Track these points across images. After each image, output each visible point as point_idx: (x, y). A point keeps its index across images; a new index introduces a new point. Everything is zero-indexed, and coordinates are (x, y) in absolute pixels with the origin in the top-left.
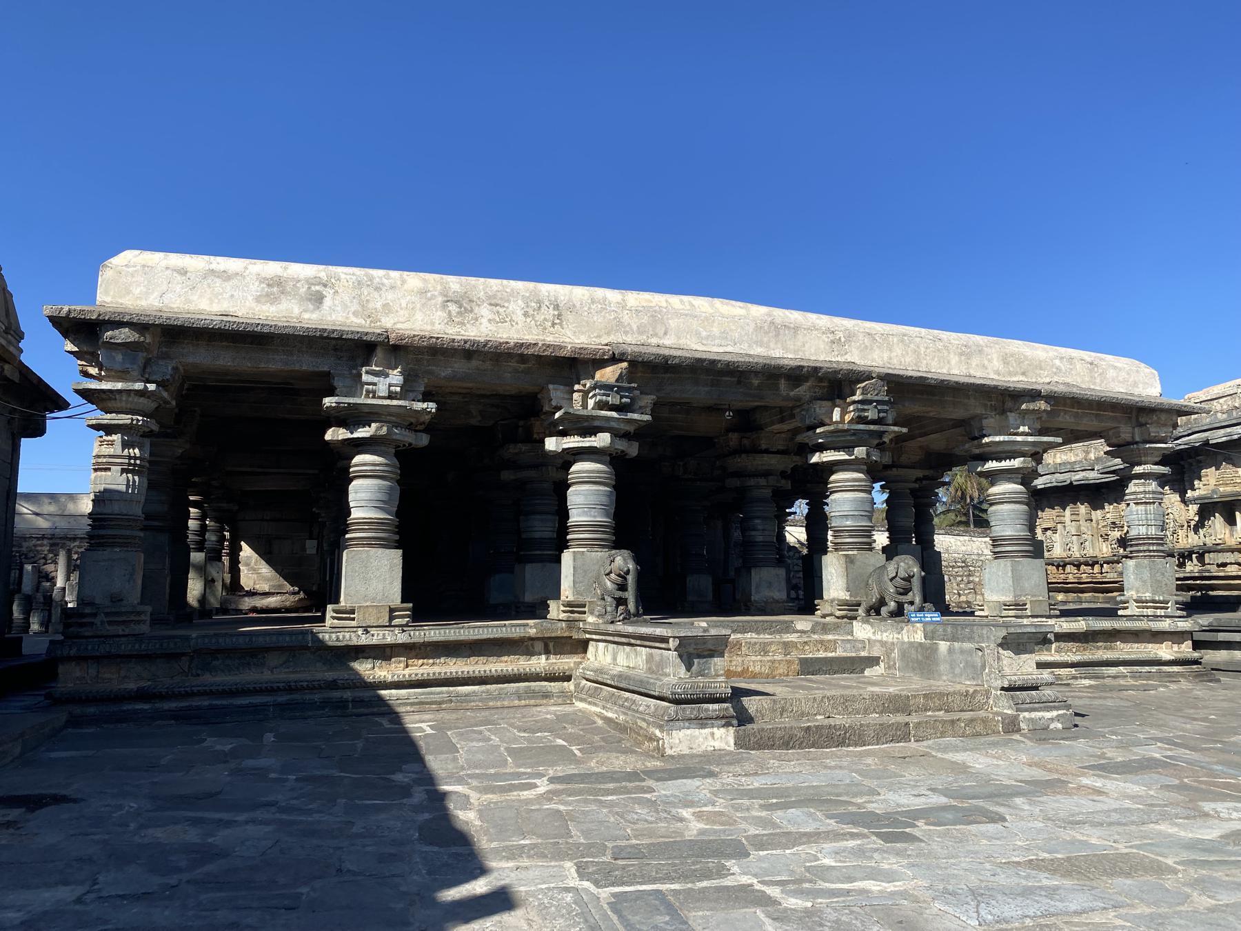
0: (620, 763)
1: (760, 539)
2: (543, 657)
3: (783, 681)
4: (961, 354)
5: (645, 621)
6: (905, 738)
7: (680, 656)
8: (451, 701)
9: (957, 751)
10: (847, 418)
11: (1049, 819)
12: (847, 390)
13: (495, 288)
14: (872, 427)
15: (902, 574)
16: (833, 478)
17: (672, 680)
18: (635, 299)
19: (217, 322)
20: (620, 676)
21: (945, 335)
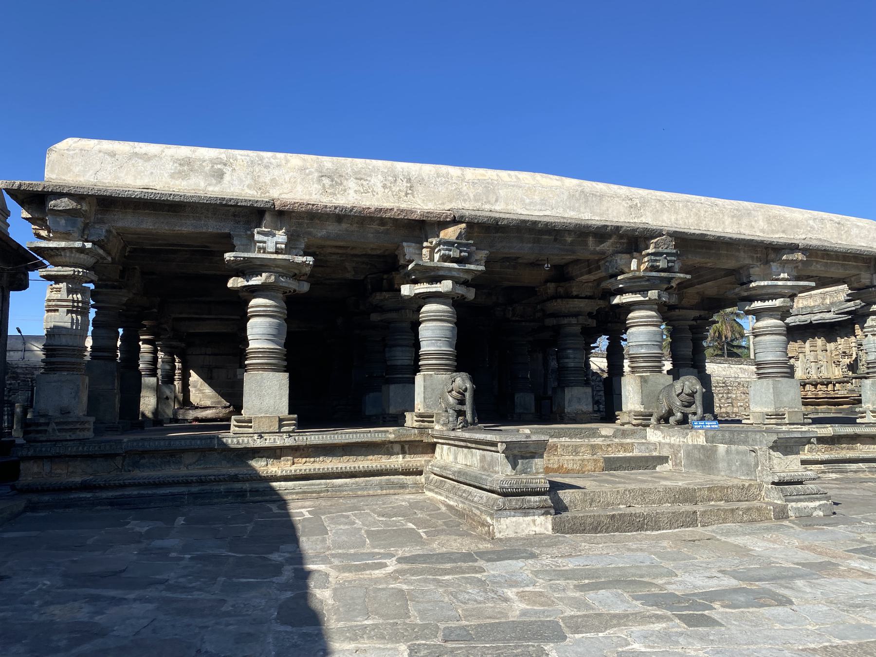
0: (457, 545)
1: (572, 365)
2: (401, 456)
3: (592, 476)
4: (733, 217)
5: (480, 428)
6: (693, 523)
7: (507, 457)
8: (328, 491)
9: (737, 535)
10: (643, 267)
11: (831, 602)
12: (642, 246)
13: (360, 166)
14: (663, 274)
15: (687, 390)
16: (631, 315)
17: (501, 476)
18: (472, 173)
19: (137, 194)
20: (459, 472)
21: (720, 201)
